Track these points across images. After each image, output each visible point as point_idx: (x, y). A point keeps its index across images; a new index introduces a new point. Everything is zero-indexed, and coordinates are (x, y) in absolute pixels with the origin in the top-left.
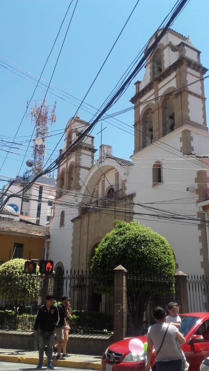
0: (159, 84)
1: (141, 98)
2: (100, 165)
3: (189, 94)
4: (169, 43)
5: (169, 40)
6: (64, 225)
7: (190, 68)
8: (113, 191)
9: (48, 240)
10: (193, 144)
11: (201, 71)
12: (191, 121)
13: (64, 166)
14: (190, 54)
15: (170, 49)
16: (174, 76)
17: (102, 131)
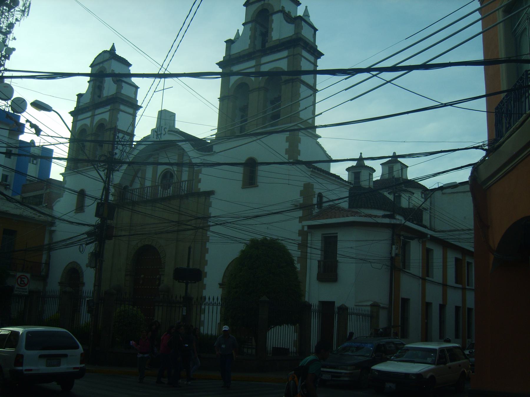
0: (262, 56)
1: (233, 65)
2: (157, 138)
3: (301, 83)
4: (281, 9)
5: (281, 6)
6: (84, 212)
7: (305, 51)
8: (172, 176)
9: (53, 228)
10: (301, 147)
11: (317, 55)
12: (300, 118)
13: (86, 120)
14: (306, 32)
15: (282, 17)
16: (286, 56)
17: (163, 90)
